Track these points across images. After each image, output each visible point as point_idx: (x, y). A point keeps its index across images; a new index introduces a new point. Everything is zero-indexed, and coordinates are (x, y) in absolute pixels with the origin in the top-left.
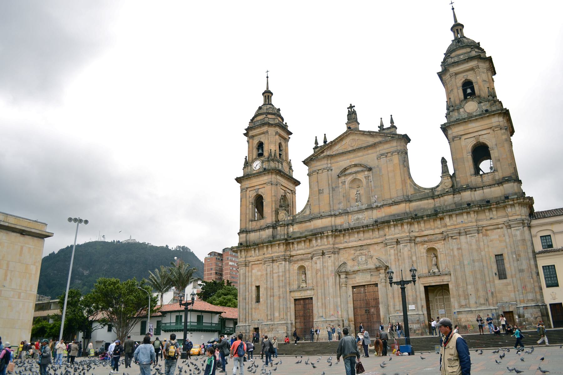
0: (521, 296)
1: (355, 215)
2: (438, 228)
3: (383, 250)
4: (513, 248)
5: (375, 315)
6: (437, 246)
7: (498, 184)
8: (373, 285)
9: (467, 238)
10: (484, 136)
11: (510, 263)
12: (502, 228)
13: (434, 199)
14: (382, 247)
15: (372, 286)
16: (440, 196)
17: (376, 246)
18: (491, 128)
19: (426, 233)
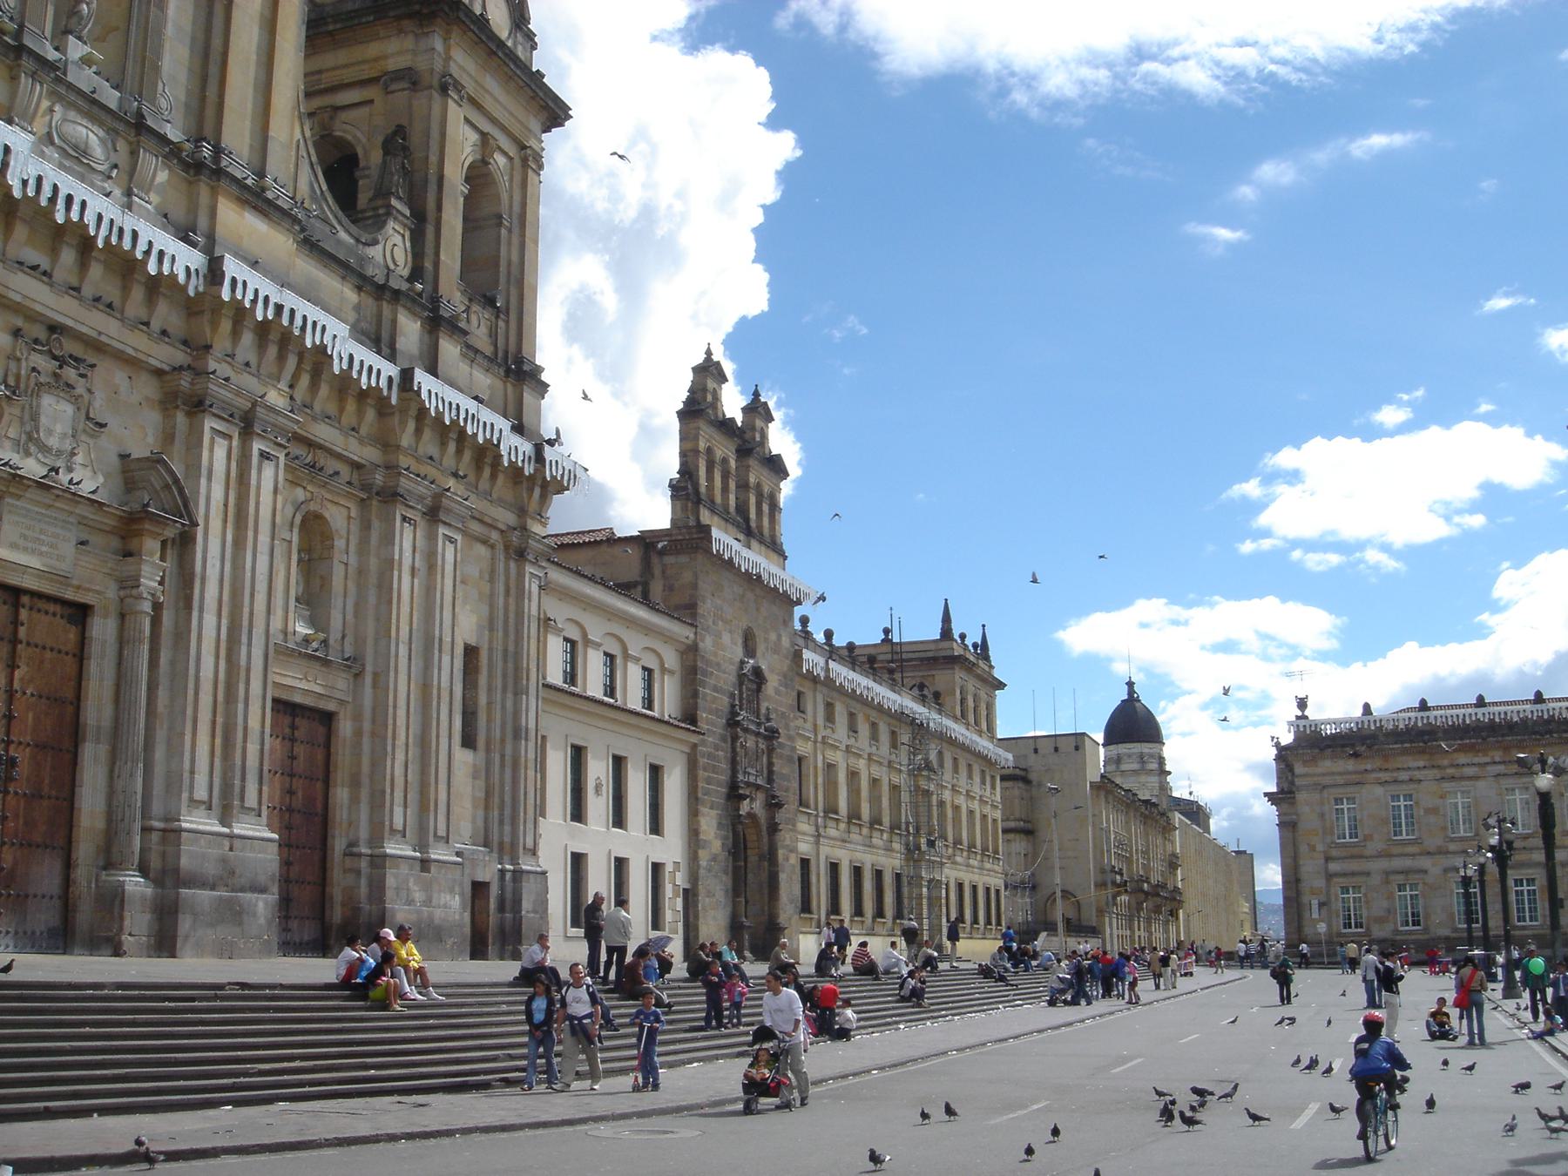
0: (507, 828)
1: (72, 115)
2: (361, 441)
3: (153, 417)
4: (512, 637)
5: (45, 803)
6: (339, 516)
7: (508, 372)
8: (58, 608)
9: (432, 538)
10: (501, 160)
11: (490, 689)
12: (492, 547)
13: (359, 289)
14: (147, 399)
15: (52, 607)
16: (388, 295)
17: (120, 377)
18: (524, 147)
19: (324, 433)
